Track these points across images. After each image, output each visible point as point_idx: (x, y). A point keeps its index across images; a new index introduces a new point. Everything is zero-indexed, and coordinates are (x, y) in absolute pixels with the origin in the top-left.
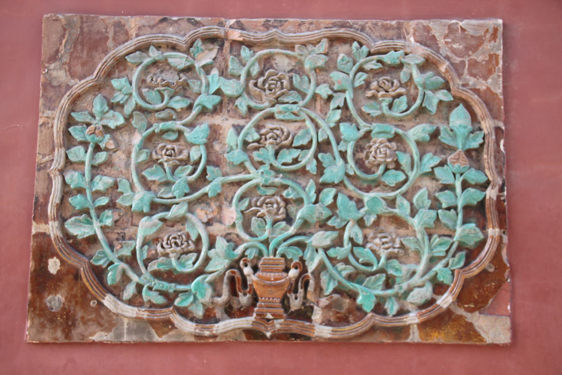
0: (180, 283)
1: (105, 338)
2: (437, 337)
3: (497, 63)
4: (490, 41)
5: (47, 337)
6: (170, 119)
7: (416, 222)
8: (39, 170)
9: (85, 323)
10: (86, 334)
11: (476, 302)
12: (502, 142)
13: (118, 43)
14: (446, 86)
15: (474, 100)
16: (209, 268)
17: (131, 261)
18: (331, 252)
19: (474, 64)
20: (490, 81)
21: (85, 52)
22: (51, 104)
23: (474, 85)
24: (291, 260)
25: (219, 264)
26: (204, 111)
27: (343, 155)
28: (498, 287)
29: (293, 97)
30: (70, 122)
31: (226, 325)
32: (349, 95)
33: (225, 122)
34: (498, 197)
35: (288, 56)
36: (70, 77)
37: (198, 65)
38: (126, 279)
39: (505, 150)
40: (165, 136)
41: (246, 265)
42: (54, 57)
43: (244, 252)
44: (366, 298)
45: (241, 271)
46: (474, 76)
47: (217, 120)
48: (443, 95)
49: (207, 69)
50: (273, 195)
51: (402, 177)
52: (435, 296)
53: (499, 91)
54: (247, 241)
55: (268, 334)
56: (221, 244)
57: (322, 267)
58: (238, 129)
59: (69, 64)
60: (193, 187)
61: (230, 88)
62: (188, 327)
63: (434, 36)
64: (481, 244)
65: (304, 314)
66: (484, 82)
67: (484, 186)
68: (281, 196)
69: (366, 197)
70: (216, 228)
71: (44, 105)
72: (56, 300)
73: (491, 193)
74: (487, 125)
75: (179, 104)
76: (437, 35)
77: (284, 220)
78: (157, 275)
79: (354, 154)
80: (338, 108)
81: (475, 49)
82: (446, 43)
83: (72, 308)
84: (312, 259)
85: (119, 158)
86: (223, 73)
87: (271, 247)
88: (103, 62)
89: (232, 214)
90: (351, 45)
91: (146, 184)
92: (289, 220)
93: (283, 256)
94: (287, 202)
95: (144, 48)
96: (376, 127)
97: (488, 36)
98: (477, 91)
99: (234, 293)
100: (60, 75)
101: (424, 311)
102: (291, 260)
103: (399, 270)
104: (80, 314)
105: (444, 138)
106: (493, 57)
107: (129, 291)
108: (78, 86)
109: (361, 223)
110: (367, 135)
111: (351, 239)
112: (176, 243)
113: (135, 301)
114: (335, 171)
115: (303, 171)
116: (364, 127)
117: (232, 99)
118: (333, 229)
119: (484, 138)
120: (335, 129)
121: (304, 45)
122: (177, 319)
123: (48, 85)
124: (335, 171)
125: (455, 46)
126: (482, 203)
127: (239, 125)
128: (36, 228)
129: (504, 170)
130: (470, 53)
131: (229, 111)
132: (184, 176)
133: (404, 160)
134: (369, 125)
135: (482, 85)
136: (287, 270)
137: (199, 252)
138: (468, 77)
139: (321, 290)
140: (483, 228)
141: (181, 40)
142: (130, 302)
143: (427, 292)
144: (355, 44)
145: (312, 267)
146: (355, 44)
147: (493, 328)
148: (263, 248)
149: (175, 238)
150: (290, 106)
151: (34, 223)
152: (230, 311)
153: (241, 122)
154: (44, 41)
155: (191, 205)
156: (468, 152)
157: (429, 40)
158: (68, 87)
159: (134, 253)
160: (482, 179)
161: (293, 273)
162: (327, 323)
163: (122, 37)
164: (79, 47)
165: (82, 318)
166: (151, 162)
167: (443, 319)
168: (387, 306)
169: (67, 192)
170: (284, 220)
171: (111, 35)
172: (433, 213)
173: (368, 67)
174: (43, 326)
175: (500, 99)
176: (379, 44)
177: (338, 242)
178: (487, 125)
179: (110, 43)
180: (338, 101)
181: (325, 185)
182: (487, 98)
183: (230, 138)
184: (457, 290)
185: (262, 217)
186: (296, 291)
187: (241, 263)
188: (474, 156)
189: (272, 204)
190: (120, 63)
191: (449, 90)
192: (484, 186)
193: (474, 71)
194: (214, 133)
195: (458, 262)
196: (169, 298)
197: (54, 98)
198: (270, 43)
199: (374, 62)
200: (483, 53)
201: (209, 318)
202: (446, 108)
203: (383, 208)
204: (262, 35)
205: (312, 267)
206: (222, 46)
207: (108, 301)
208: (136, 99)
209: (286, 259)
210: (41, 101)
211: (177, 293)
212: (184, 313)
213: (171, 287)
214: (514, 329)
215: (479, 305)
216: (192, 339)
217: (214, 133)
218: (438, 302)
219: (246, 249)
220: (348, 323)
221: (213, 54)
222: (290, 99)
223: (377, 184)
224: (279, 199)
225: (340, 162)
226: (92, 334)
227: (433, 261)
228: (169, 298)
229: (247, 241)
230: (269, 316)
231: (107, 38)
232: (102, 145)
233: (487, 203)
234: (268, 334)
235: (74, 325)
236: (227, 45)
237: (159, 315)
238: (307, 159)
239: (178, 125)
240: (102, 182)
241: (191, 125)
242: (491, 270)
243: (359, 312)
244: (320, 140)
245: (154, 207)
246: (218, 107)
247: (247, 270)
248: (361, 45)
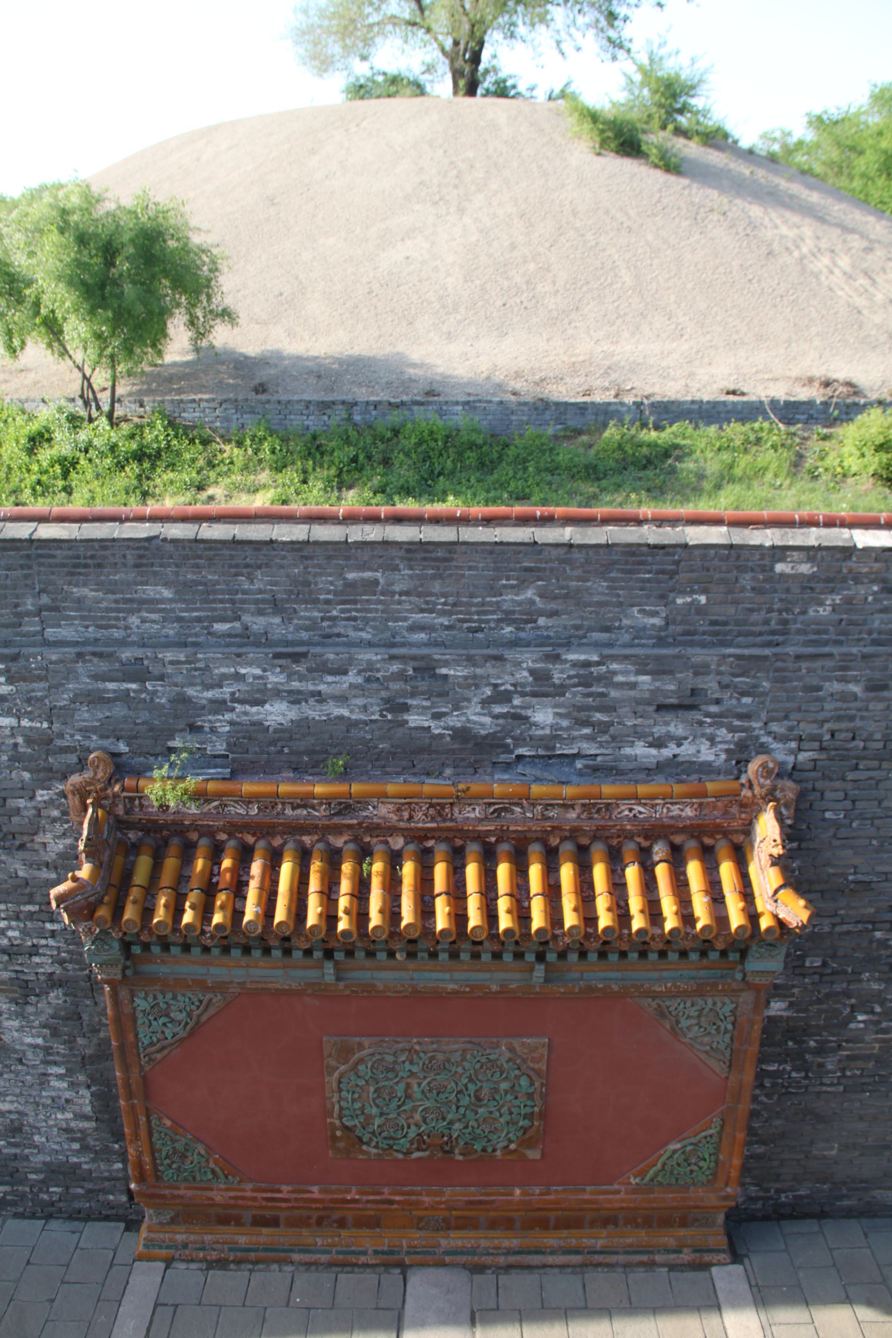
7: (502, 1120)
13: (359, 1051)
14: (519, 1069)
15: (532, 1073)
19: (533, 1058)
22: (330, 1074)
25: (412, 1135)
27: (469, 1095)
29: (446, 1072)
30: (340, 1082)
31: (416, 1155)
32: (472, 1072)
33: (414, 1082)
38: (371, 1139)
42: (330, 1056)
44: (478, 1147)
47: (409, 1080)
48: (517, 1072)
49: (404, 1062)
53: (544, 1068)
56: (413, 1128)
58: (419, 1084)
60: (399, 1107)
61: (415, 1069)
62: (400, 1156)
65: (451, 1152)
67: (532, 1107)
70: (411, 1121)
73: (536, 1109)
74: (537, 1084)
75: (390, 1075)
85: (364, 1095)
86: (412, 1063)
89: (418, 1117)
91: (377, 1106)
92: (444, 1119)
95: (372, 1055)
96: (484, 1085)
98: (533, 1069)
100: (333, 1063)
103: (493, 1137)
105: (517, 1088)
106: (542, 1055)
107: (374, 1144)
109: (477, 1120)
110: (481, 1087)
113: (376, 1147)
114: (465, 1101)
123: (328, 1067)
124: (465, 1101)
126: (532, 1113)
128: (328, 1120)
132: (394, 1103)
133: (497, 1097)
135: (536, 1066)
147: (533, 1154)
155: (399, 1114)
156: (528, 1094)
157: (512, 1049)
160: (532, 1104)
161: (445, 1139)
162: (461, 1154)
166: (379, 1097)
169: (341, 1109)
176: (488, 1051)
177: (466, 1127)
178: (537, 1084)
180: (468, 1074)
182: (538, 1072)
183: (415, 1087)
188: (530, 1096)
190: (361, 1061)
192: (532, 1107)
194: (408, 1086)
195: (520, 1134)
196: (391, 1147)
198: (435, 1051)
202: (517, 1078)
203: (487, 1115)
205: (455, 1136)
207: (364, 1147)
208: (370, 1074)
213: (391, 1142)
214: (543, 1155)
217: (408, 1086)
225: (467, 1098)
227: (508, 1133)
228: (391, 1147)
240: (357, 1105)
241: (397, 1083)
245: (382, 1114)
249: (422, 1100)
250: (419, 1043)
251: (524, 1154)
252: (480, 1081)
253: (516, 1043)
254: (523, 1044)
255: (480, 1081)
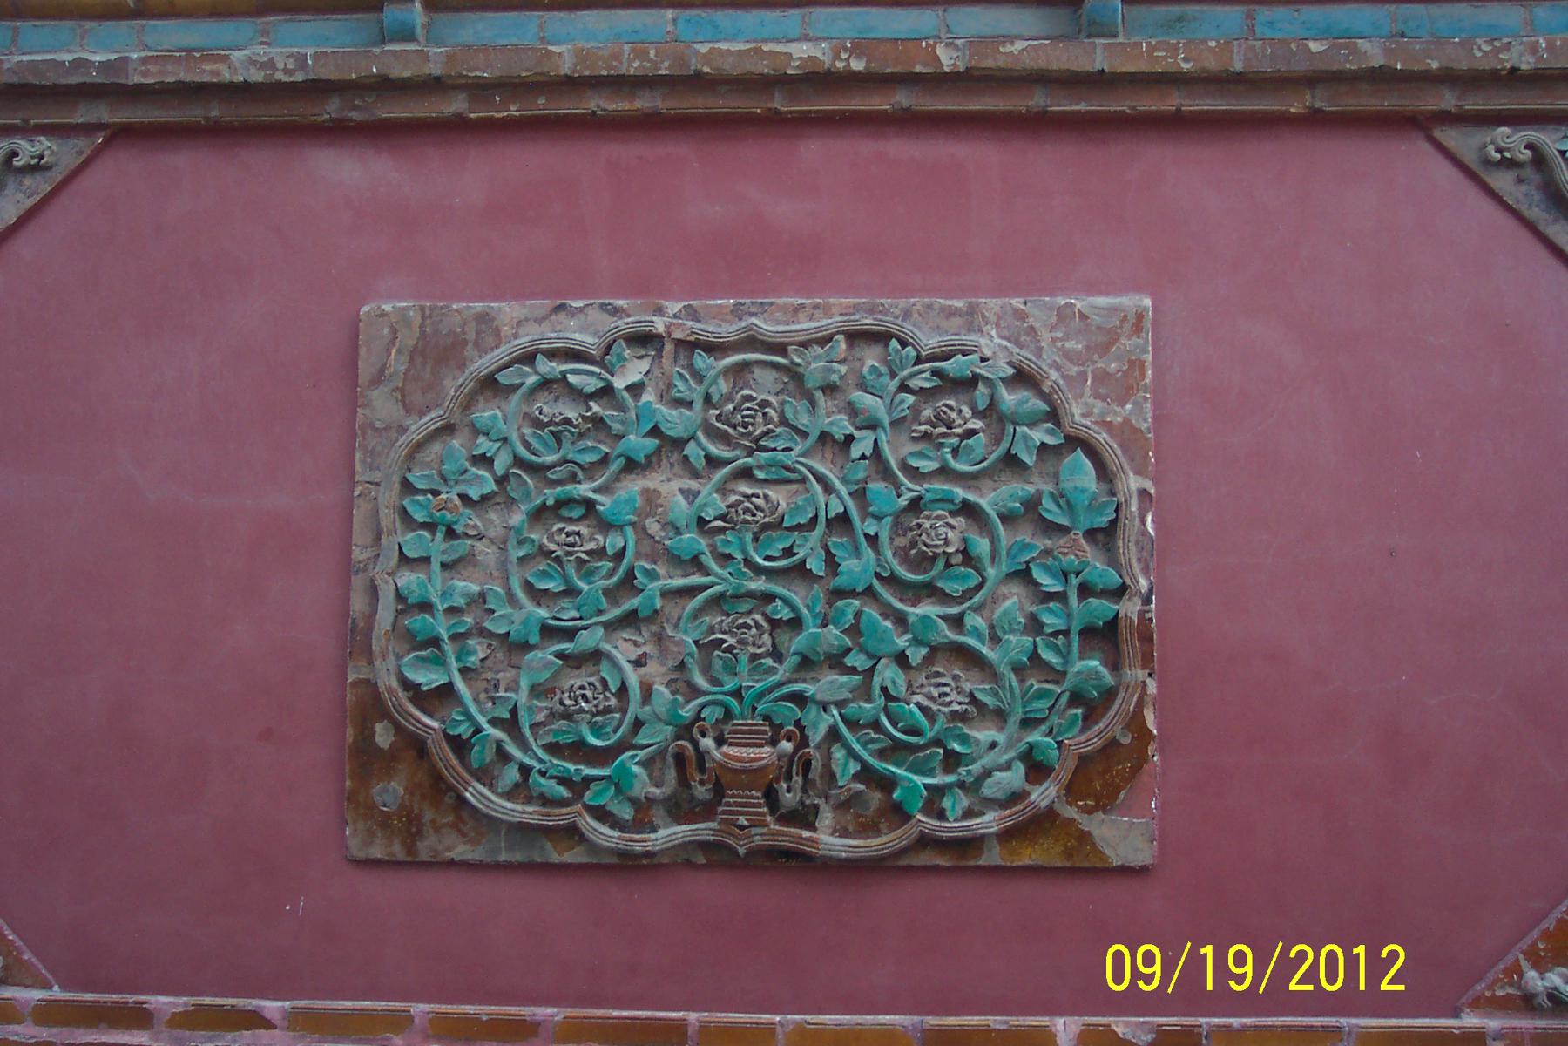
0: (590, 764)
1: (469, 857)
2: (1029, 856)
3: (1143, 375)
4: (1129, 337)
5: (377, 852)
6: (573, 478)
8: (357, 573)
9: (437, 830)
10: (440, 848)
11: (1098, 797)
12: (1149, 518)
13: (483, 351)
16: (640, 739)
17: (511, 724)
18: (851, 709)
19: (1102, 377)
20: (1129, 407)
21: (428, 369)
23: (1102, 414)
24: (781, 726)
25: (656, 736)
26: (631, 466)
27: (873, 540)
28: (1136, 769)
31: (667, 834)
34: (1141, 614)
35: (774, 365)
36: (402, 412)
37: (619, 383)
39: (1156, 530)
40: (565, 512)
41: (704, 735)
42: (378, 379)
43: (700, 712)
45: (695, 743)
46: (1103, 398)
47: (654, 481)
49: (636, 389)
50: (749, 613)
51: (975, 580)
52: (1028, 787)
54: (705, 693)
55: (742, 851)
57: (833, 735)
58: (690, 495)
59: (402, 390)
61: (675, 421)
62: (606, 835)
63: (1032, 328)
64: (1109, 694)
66: (1118, 409)
67: (1120, 592)
68: (764, 615)
69: (915, 612)
71: (363, 462)
72: (391, 792)
76: (1037, 325)
77: (768, 654)
78: (553, 748)
79: (891, 539)
80: (863, 457)
81: (1104, 349)
82: (1054, 340)
83: (416, 806)
84: (815, 726)
87: (747, 703)
88: (454, 384)
90: (887, 345)
93: (766, 718)
94: (775, 624)
95: (529, 358)
97: (1127, 327)
98: (1108, 426)
99: (683, 781)
101: (1007, 812)
102: (781, 726)
104: (428, 815)
108: (418, 427)
111: (884, 690)
112: (584, 696)
115: (800, 570)
116: (910, 489)
117: (679, 443)
118: (853, 671)
119: (1116, 511)
120: (860, 495)
121: (805, 345)
122: (589, 824)
124: (856, 568)
125: (1070, 345)
126: (1113, 624)
127: (689, 490)
129: (1152, 565)
130: (1096, 357)
131: (672, 465)
134: (917, 488)
136: (773, 742)
137: (624, 711)
138: (1091, 400)
139: (833, 776)
140: (1115, 666)
141: (587, 340)
142: (509, 795)
143: (1015, 777)
144: (894, 343)
145: (817, 735)
146: (894, 343)
148: (733, 703)
149: (582, 688)
150: (781, 456)
151: (351, 665)
152: (681, 810)
153: (693, 484)
154: (363, 352)
156: (1091, 534)
158: (402, 430)
159: (514, 712)
160: (1113, 579)
163: (490, 340)
164: (419, 360)
165: (433, 821)
167: (1041, 823)
168: (947, 803)
170: (768, 654)
171: (471, 336)
172: (1027, 640)
173: (916, 383)
174: (371, 833)
175: (1147, 439)
179: (470, 351)
181: (840, 593)
182: (1127, 434)
184: (1065, 777)
185: (730, 649)
186: (789, 778)
187: (695, 730)
189: (746, 626)
190: (490, 385)
191: (1058, 424)
192: (1120, 592)
193: (1102, 391)
197: (379, 448)
199: (927, 375)
200: (1118, 359)
201: (643, 823)
204: (728, 330)
205: (817, 735)
206: (660, 351)
209: (772, 725)
210: (358, 456)
211: (588, 780)
212: (601, 814)
215: (1104, 802)
216: (614, 860)
218: (1033, 797)
219: (703, 706)
220: (879, 833)
221: (644, 365)
222: (781, 444)
223: (931, 591)
224: (758, 617)
225: (869, 553)
226: (449, 849)
228: (578, 787)
229: (705, 693)
230: (742, 821)
231: (465, 342)
232: (459, 528)
233: (1122, 624)
234: (742, 851)
235: (419, 833)
236: (669, 347)
237: (558, 817)
238: (810, 551)
239: (584, 489)
242: (1126, 741)
243: (899, 814)
244: (831, 514)
246: (654, 460)
247: (707, 743)
248: (904, 344)
249: (696, 564)
250: (693, 314)
251: (1085, 837)
252: (914, 474)
253: (1039, 311)
254: (1064, 315)
255: (914, 474)
